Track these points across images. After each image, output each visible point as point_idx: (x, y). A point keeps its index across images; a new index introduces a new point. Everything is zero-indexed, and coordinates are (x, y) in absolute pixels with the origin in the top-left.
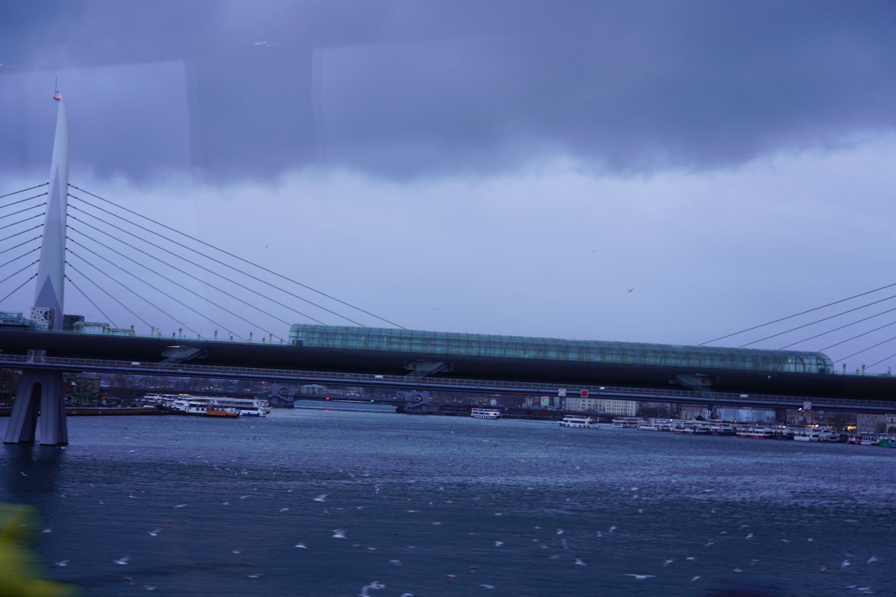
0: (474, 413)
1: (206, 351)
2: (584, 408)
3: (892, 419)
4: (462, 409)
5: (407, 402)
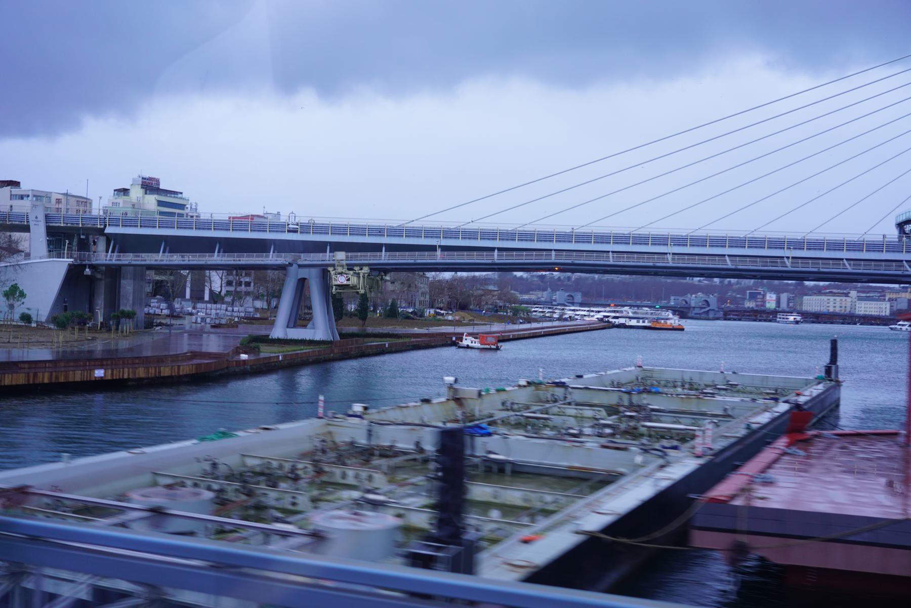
0: (780, 318)
4: (748, 314)
5: (694, 308)
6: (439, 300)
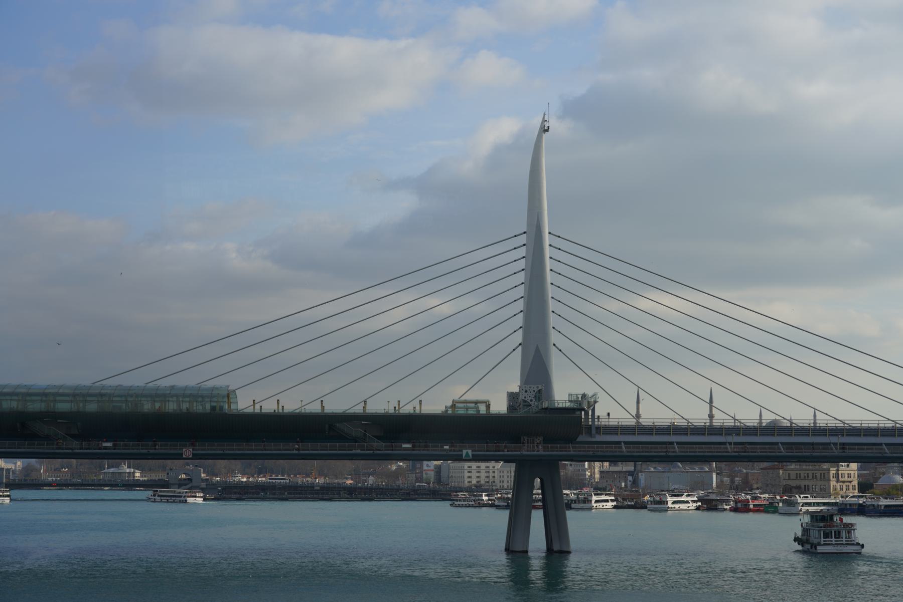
2: (471, 482)
3: (789, 474)
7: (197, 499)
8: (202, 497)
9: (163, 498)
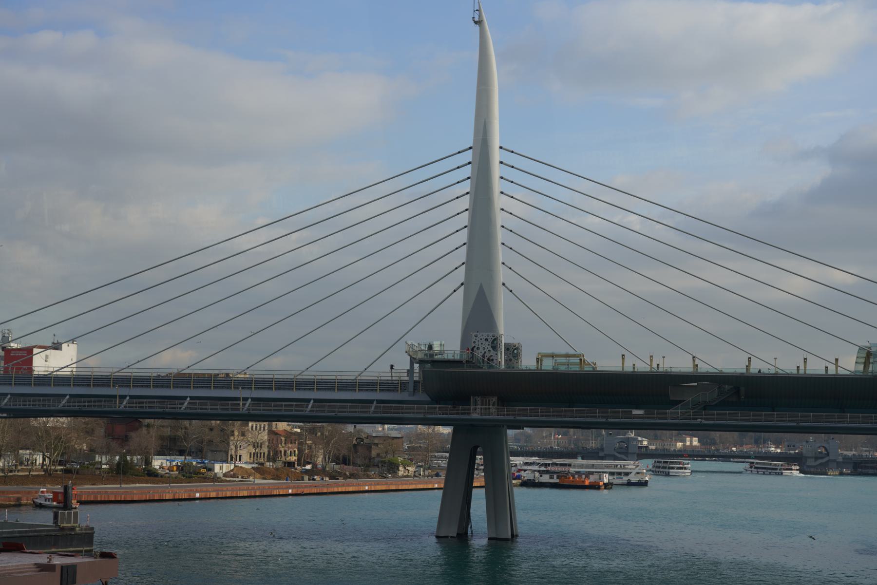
1: (743, 389)
6: (289, 452)
7: (792, 472)
8: (797, 470)
9: (759, 470)
